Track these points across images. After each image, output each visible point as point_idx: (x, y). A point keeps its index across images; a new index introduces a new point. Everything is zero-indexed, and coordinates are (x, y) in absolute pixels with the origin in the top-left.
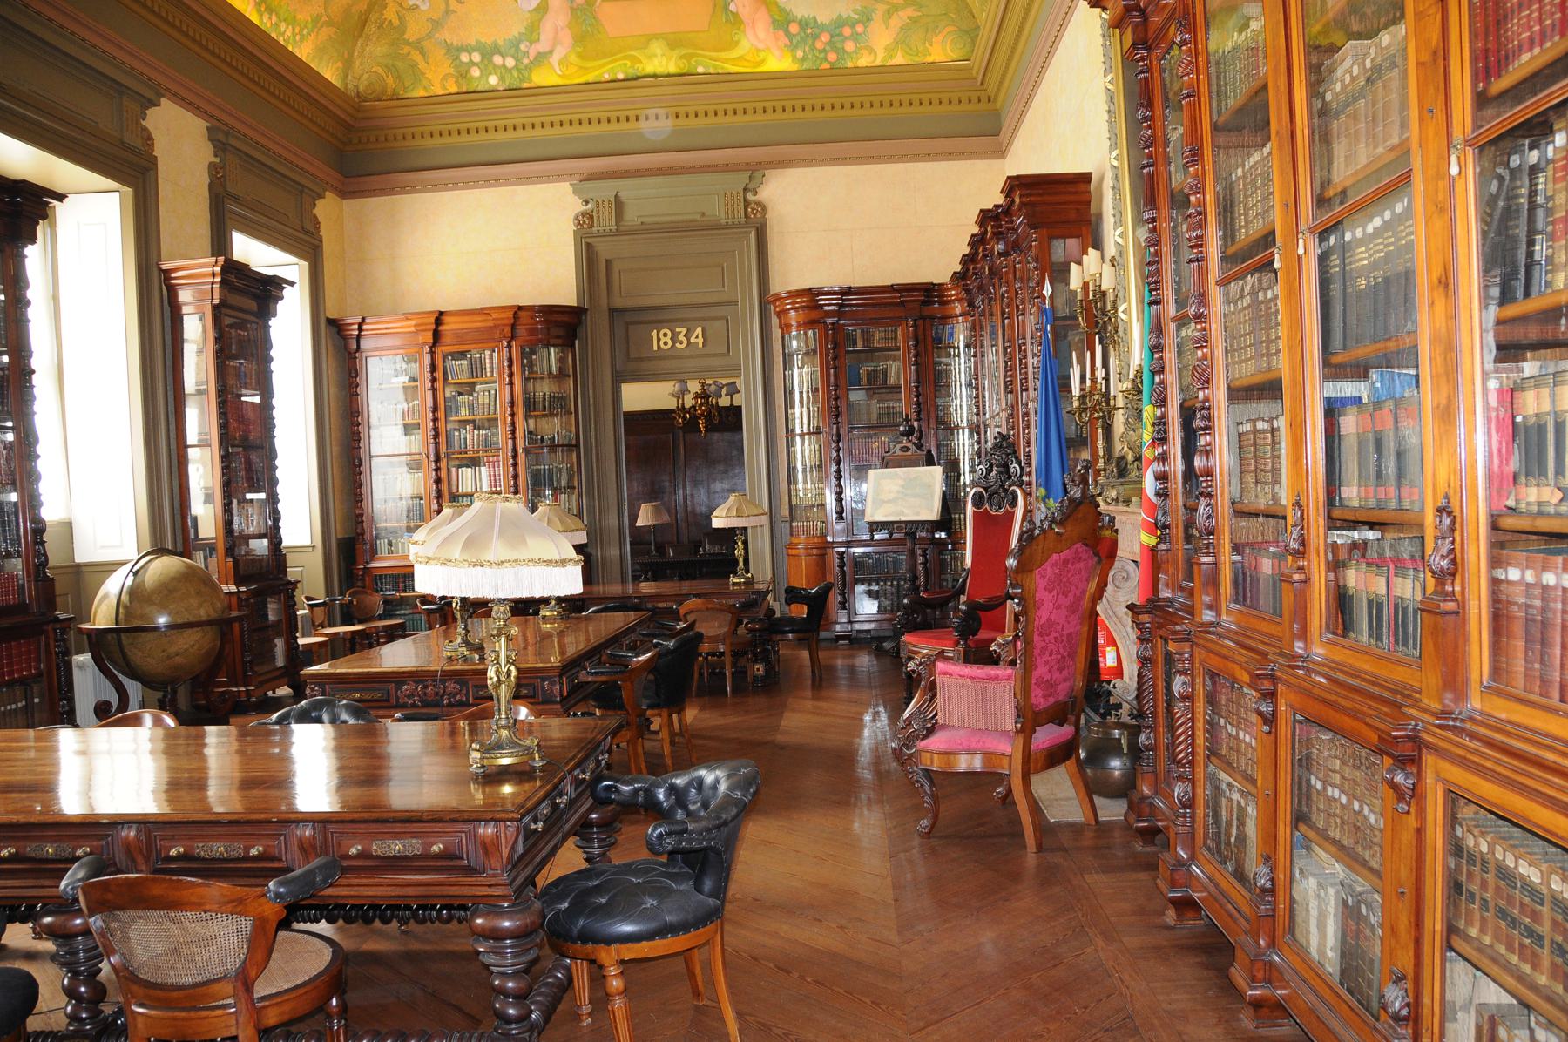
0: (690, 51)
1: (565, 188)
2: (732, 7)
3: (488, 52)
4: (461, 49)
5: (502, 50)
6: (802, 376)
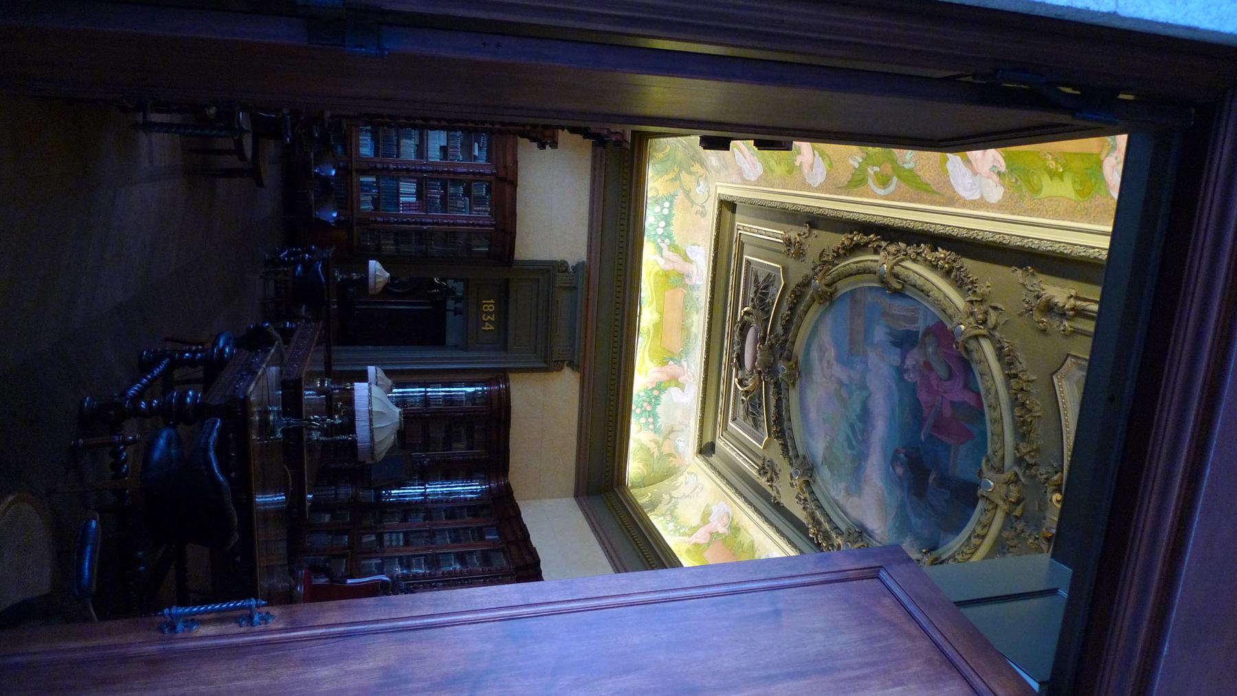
2: (671, 362)
3: (667, 219)
4: (671, 202)
5: (667, 228)
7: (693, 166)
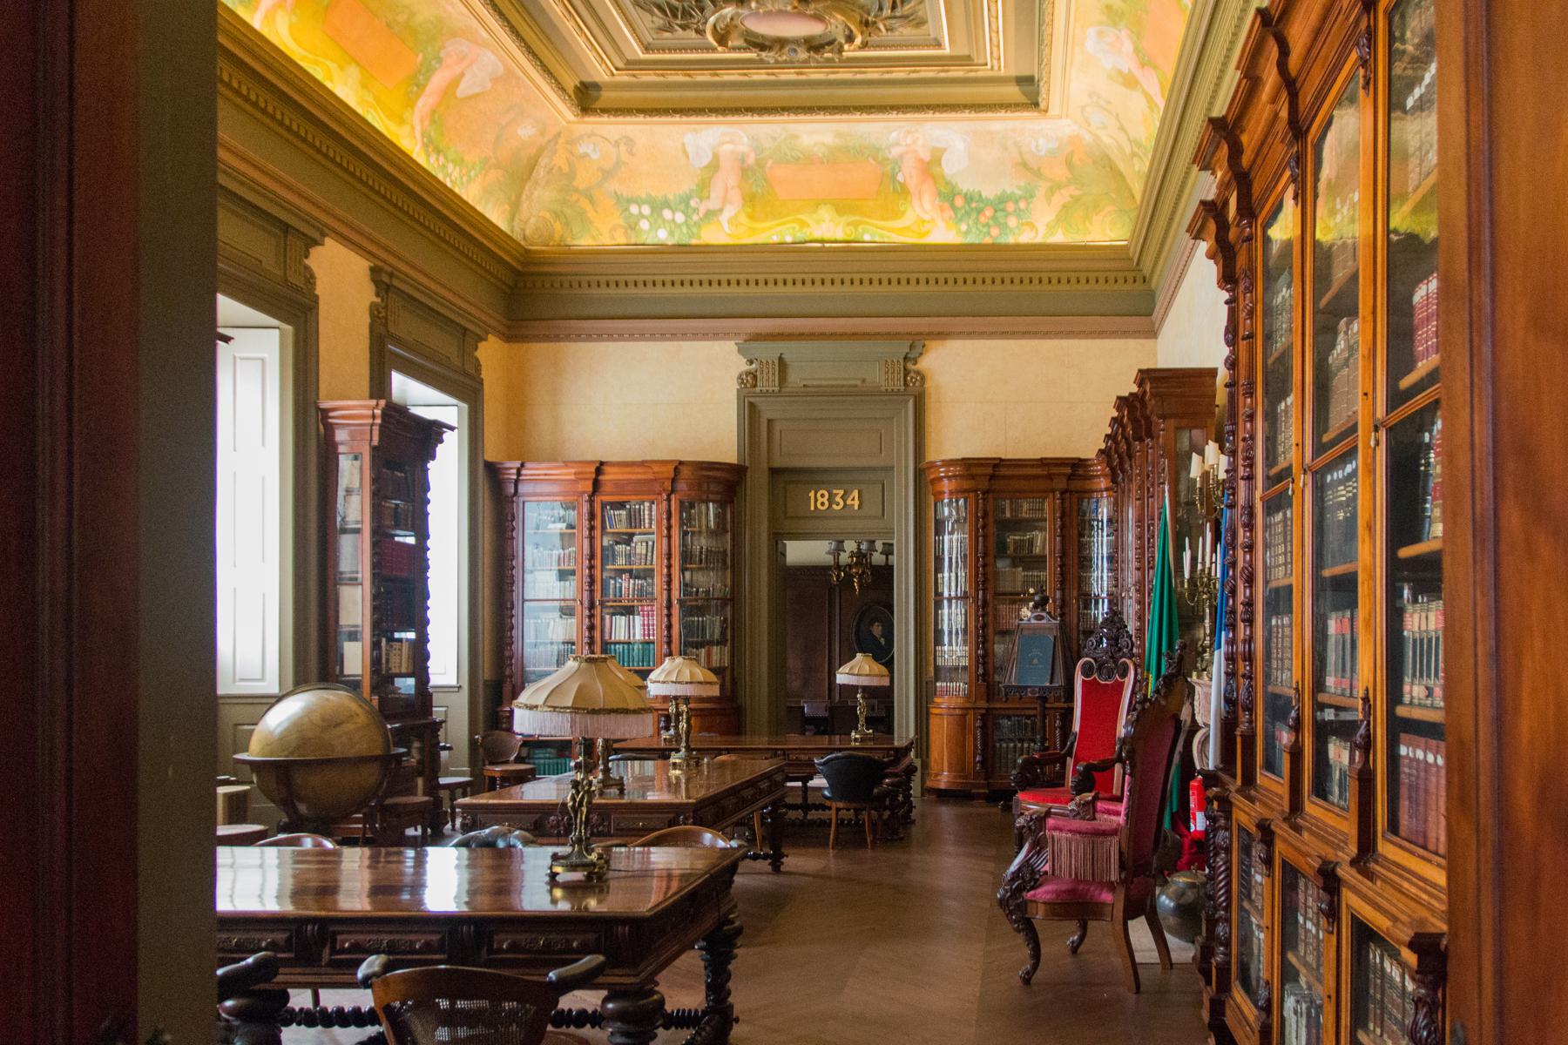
0: (858, 218)
1: (728, 348)
2: (900, 178)
3: (658, 206)
4: (629, 201)
5: (672, 205)
6: (953, 542)
7: (560, 168)
